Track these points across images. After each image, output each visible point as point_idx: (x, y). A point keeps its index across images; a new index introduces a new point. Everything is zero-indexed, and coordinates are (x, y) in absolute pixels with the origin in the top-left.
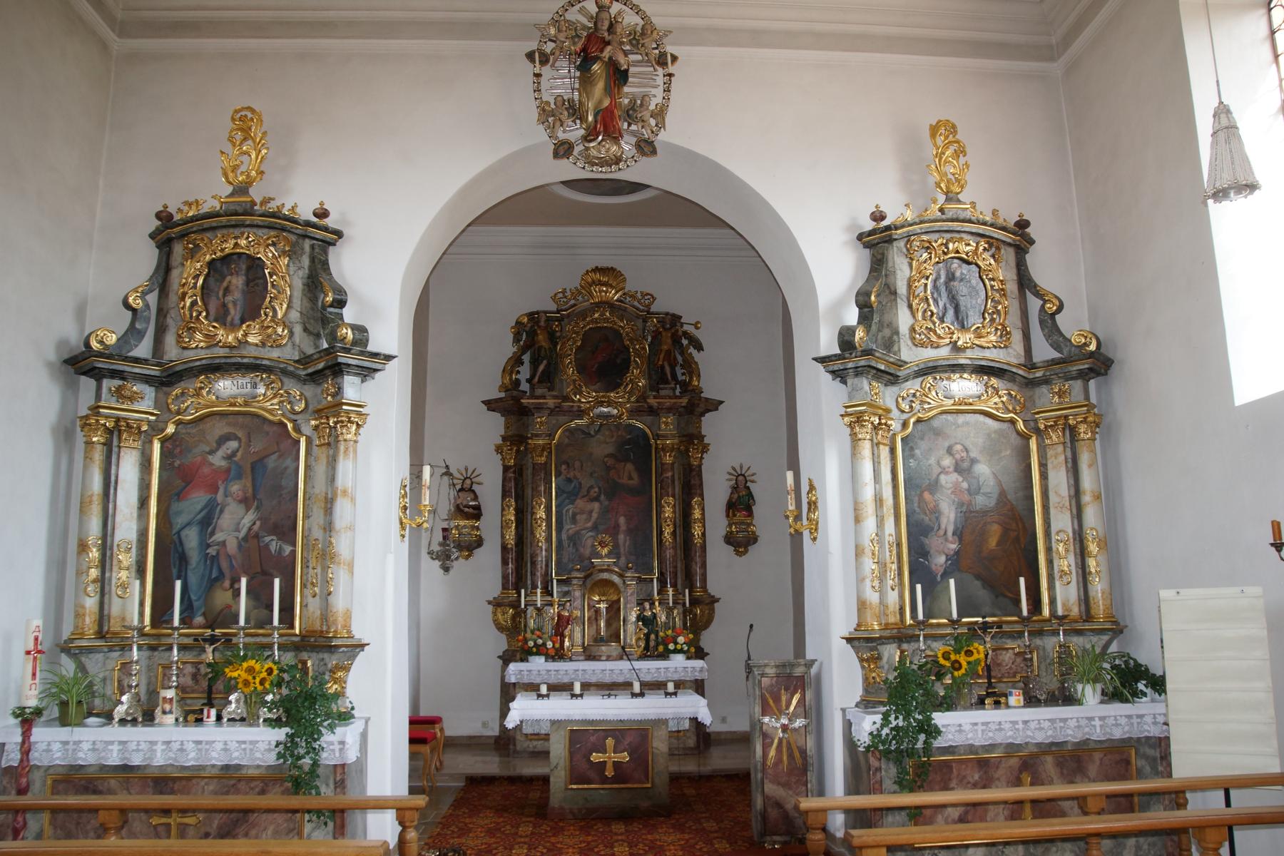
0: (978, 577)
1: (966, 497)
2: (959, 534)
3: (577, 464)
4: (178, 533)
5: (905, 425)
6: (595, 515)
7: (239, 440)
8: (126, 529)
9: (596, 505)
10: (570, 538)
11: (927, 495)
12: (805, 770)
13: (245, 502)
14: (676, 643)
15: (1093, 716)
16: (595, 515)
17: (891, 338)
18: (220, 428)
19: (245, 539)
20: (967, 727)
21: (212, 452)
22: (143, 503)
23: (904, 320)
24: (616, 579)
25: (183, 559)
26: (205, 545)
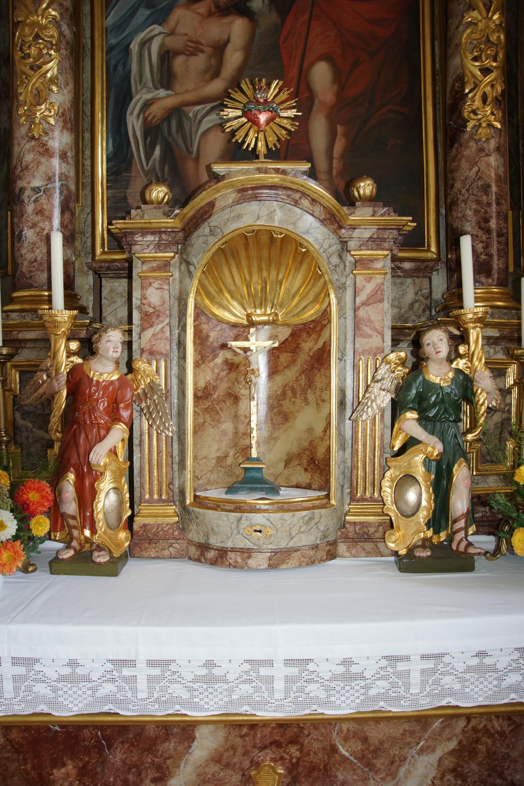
6: (233, 59)
9: (238, 28)
10: (151, 131)
16: (233, 59)
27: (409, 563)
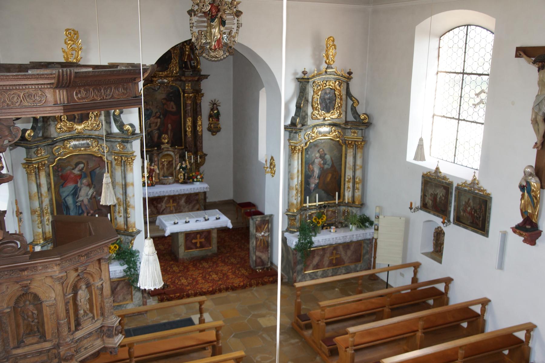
0: (323, 190)
1: (322, 166)
2: (319, 177)
3: (151, 103)
4: (64, 199)
5: (306, 144)
7: (84, 164)
8: (46, 202)
9: (159, 120)
11: (311, 166)
12: (268, 247)
13: (89, 186)
14: (197, 179)
15: (353, 234)
16: (158, 124)
17: (305, 116)
18: (75, 161)
19: (91, 198)
20: (320, 241)
21: (73, 169)
22: (49, 189)
23: (310, 110)
24: (172, 153)
25: (67, 208)
26: (75, 202)
27: (182, 183)
